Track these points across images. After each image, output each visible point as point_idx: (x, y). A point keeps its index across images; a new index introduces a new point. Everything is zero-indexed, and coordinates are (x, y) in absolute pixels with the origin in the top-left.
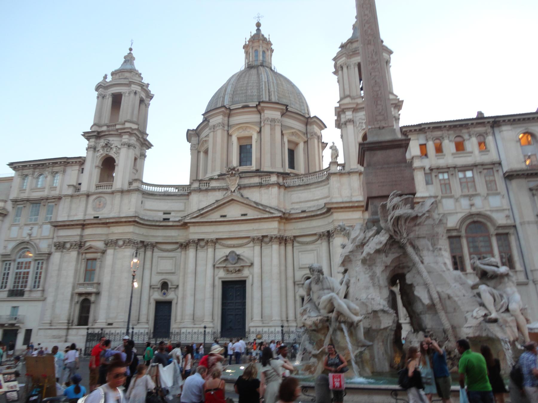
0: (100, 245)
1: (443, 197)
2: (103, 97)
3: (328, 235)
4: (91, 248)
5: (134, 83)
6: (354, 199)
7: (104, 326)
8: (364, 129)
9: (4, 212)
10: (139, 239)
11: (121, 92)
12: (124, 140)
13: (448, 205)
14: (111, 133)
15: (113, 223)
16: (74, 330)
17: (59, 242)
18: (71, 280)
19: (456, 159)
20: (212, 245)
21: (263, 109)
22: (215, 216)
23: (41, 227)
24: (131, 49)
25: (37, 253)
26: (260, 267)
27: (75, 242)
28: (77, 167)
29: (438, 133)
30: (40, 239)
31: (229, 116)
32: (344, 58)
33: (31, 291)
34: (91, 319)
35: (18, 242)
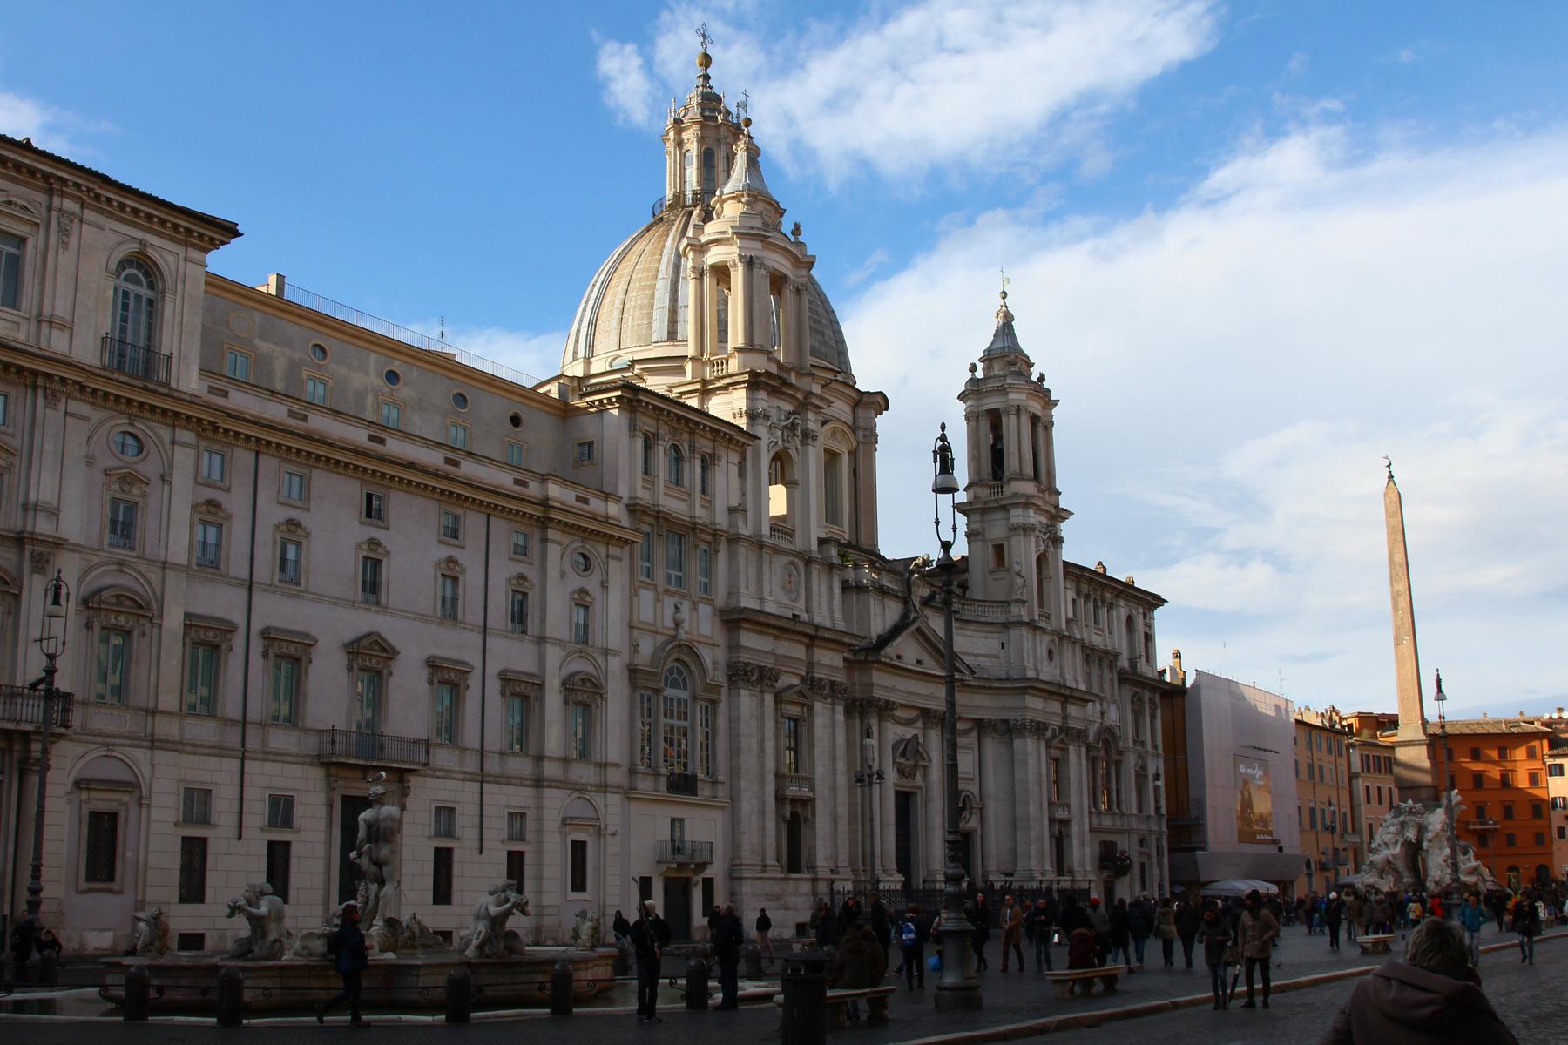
3: (1008, 730)
6: (1042, 677)
7: (828, 875)
11: (786, 276)
13: (1090, 704)
15: (823, 639)
16: (791, 882)
18: (770, 764)
21: (869, 405)
23: (695, 609)
25: (708, 681)
29: (1085, 588)
30: (698, 642)
32: (1024, 397)
34: (803, 863)
35: (660, 639)
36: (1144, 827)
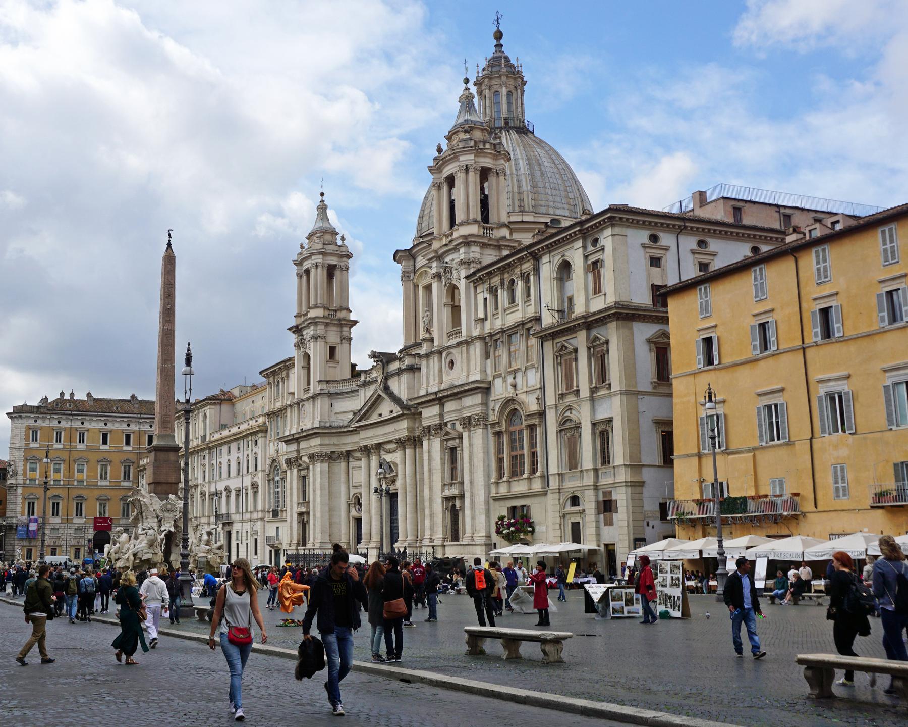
0: (305, 459)
1: (494, 377)
2: (301, 276)
4: (300, 465)
5: (312, 254)
8: (445, 285)
9: (262, 428)
10: (329, 451)
12: (312, 333)
14: (303, 325)
17: (287, 459)
19: (508, 316)
20: (375, 452)
22: (374, 418)
24: (322, 194)
26: (404, 476)
27: (294, 458)
28: (293, 369)
31: (414, 258)
33: (282, 511)
36: (571, 485)
